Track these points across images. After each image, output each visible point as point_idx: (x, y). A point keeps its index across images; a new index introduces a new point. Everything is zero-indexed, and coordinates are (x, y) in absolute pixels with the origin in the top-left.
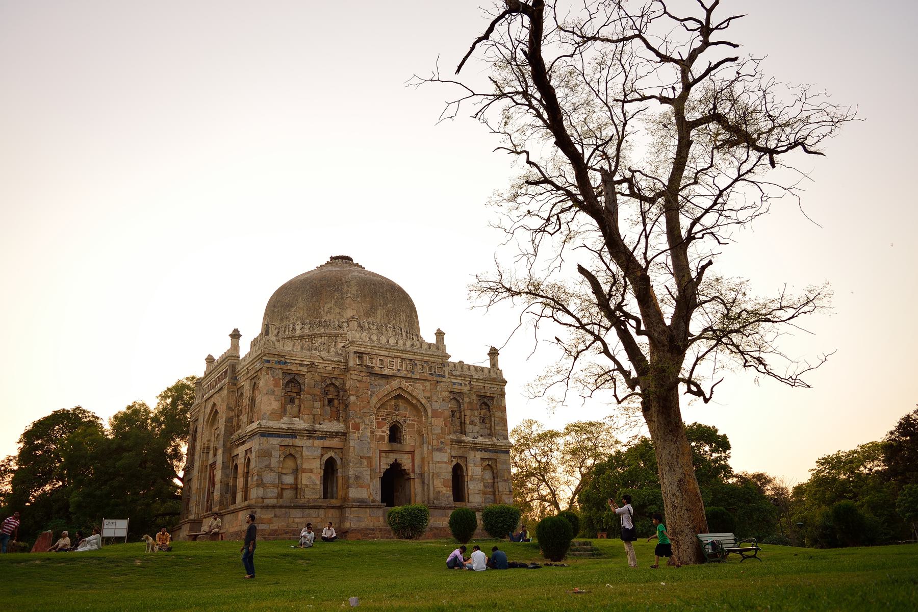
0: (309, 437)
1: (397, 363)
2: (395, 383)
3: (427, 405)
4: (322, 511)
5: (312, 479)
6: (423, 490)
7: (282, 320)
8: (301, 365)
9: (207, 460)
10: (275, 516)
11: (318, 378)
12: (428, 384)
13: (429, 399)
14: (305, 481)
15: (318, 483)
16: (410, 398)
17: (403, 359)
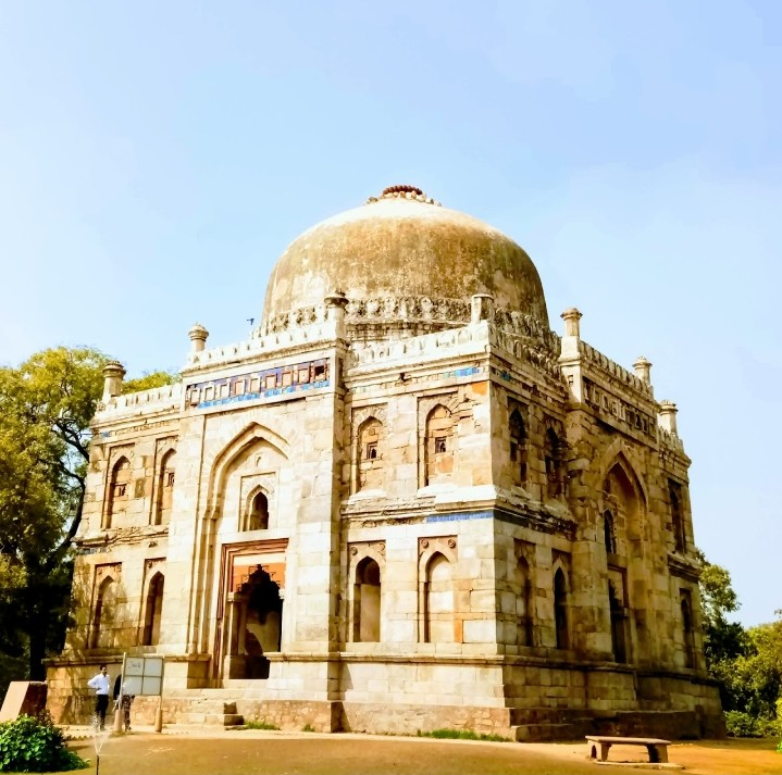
0: (544, 530)
1: (620, 412)
2: (618, 444)
3: (644, 488)
4: (568, 672)
5: (544, 608)
6: (642, 639)
7: (372, 286)
8: (525, 387)
9: (214, 534)
10: (527, 683)
11: (540, 416)
12: (643, 450)
13: (644, 476)
14: (541, 615)
15: (552, 616)
16: (627, 473)
17: (623, 402)
